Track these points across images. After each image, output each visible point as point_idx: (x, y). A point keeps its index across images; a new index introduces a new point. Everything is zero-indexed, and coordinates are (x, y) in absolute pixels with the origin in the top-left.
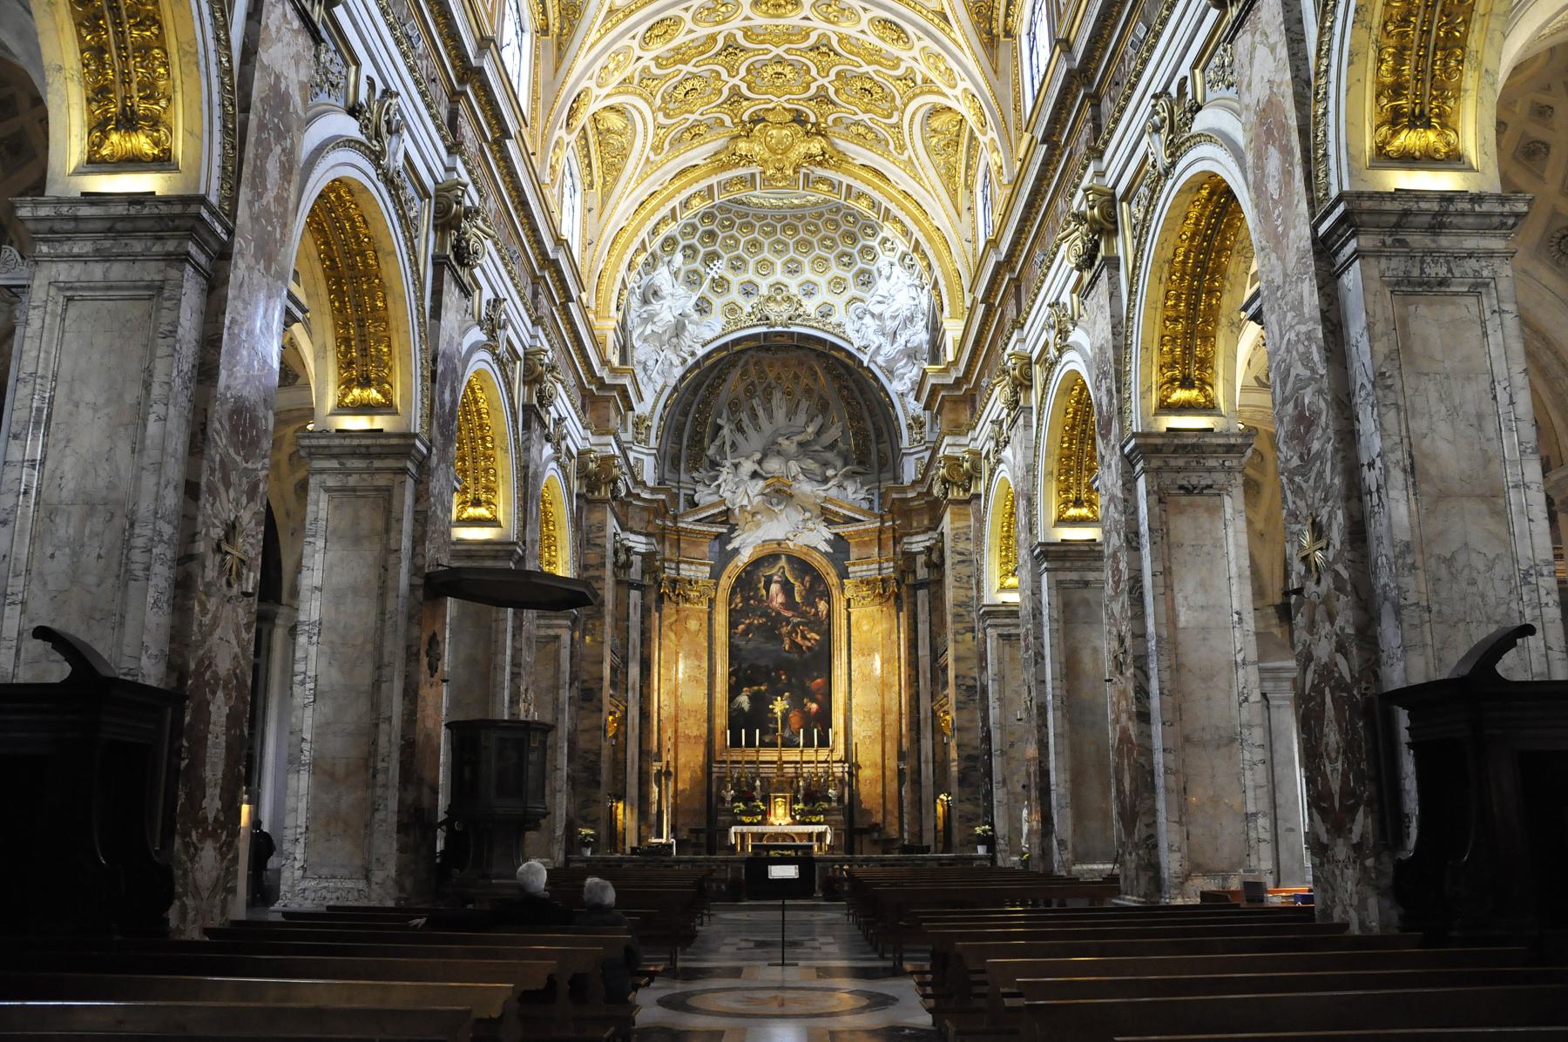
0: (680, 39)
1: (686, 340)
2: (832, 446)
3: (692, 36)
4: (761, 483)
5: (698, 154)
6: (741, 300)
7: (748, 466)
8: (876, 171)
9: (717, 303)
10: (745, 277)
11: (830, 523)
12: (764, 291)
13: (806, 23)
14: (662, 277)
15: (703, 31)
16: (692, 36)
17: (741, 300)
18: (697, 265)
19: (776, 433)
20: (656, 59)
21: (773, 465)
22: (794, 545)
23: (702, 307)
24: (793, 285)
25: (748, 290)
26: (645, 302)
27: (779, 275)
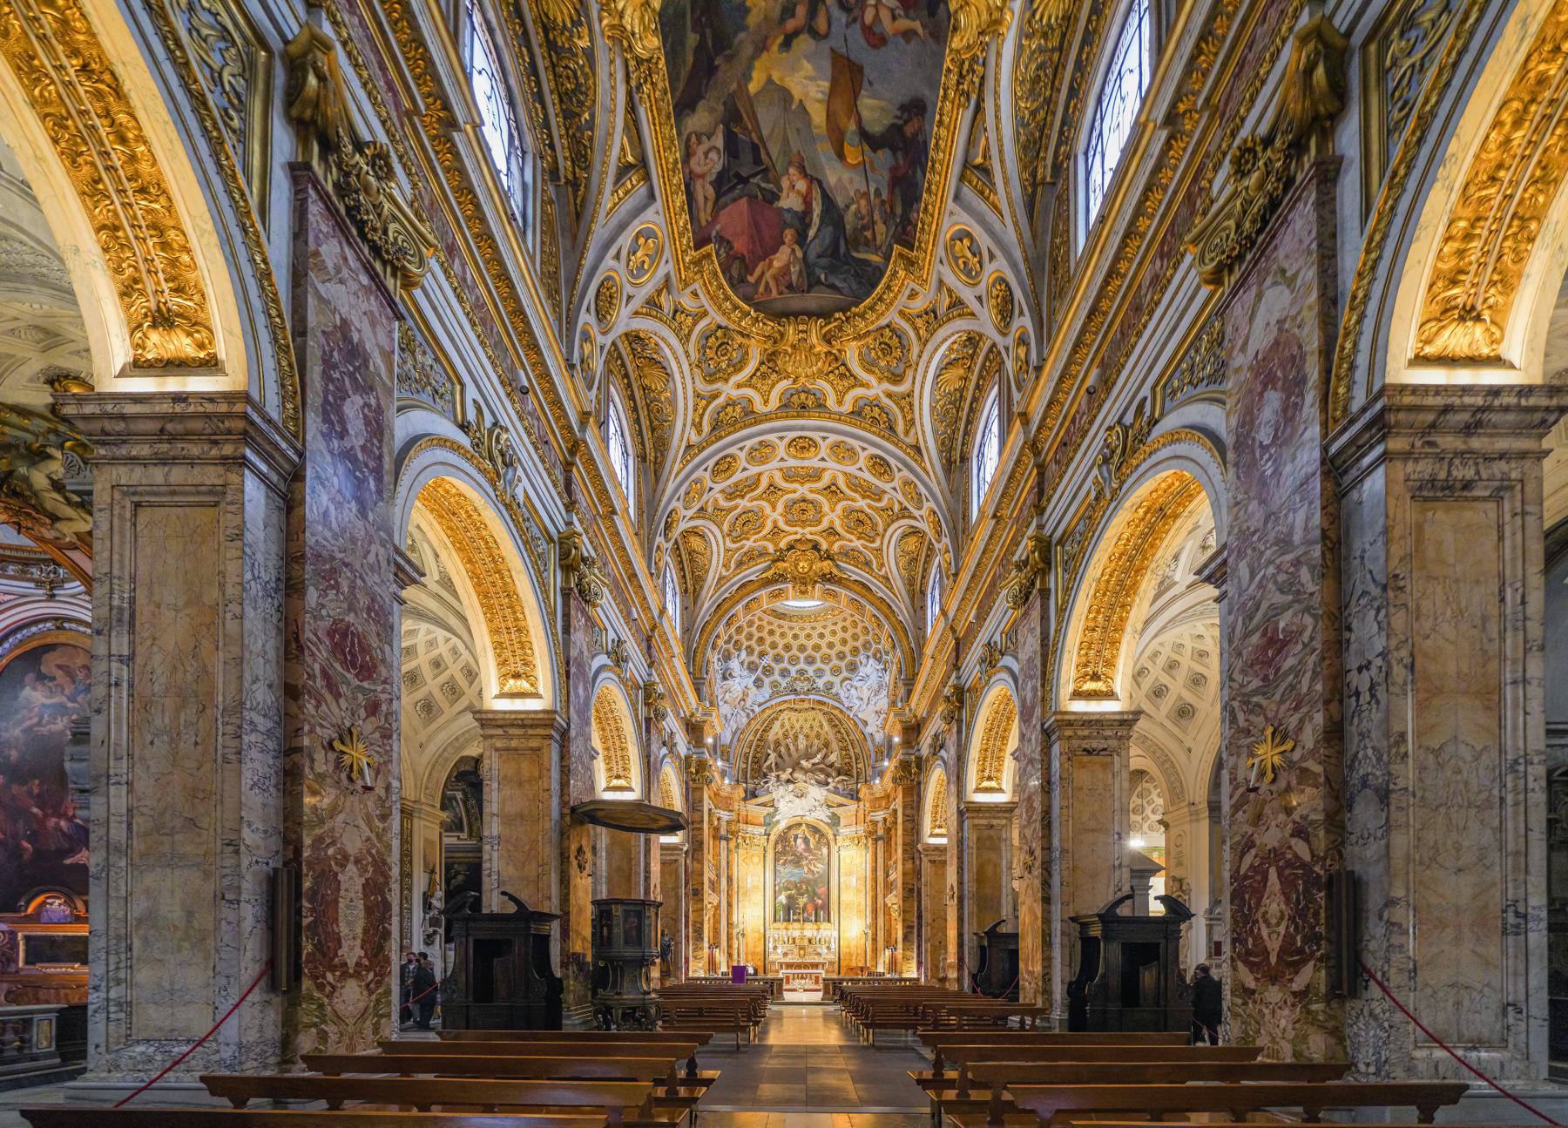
0: (738, 476)
1: (749, 702)
2: (831, 766)
3: (746, 474)
4: (791, 787)
5: (752, 572)
6: (779, 679)
7: (784, 776)
8: (864, 585)
9: (767, 681)
10: (782, 666)
11: (829, 806)
12: (793, 674)
13: (822, 464)
14: (734, 664)
15: (754, 470)
16: (746, 474)
17: (779, 679)
18: (754, 658)
19: (800, 758)
20: (722, 491)
21: (798, 775)
22: (809, 819)
23: (758, 683)
24: (810, 670)
25: (784, 673)
26: (725, 678)
27: (802, 665)
